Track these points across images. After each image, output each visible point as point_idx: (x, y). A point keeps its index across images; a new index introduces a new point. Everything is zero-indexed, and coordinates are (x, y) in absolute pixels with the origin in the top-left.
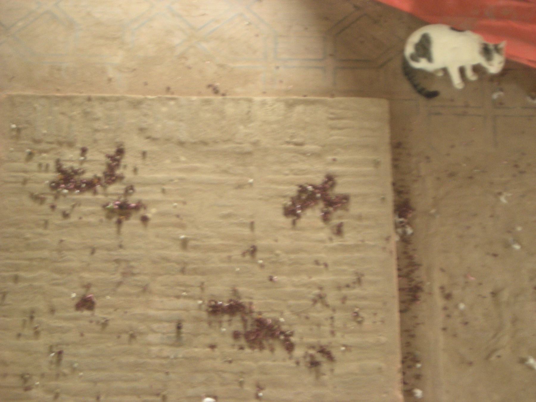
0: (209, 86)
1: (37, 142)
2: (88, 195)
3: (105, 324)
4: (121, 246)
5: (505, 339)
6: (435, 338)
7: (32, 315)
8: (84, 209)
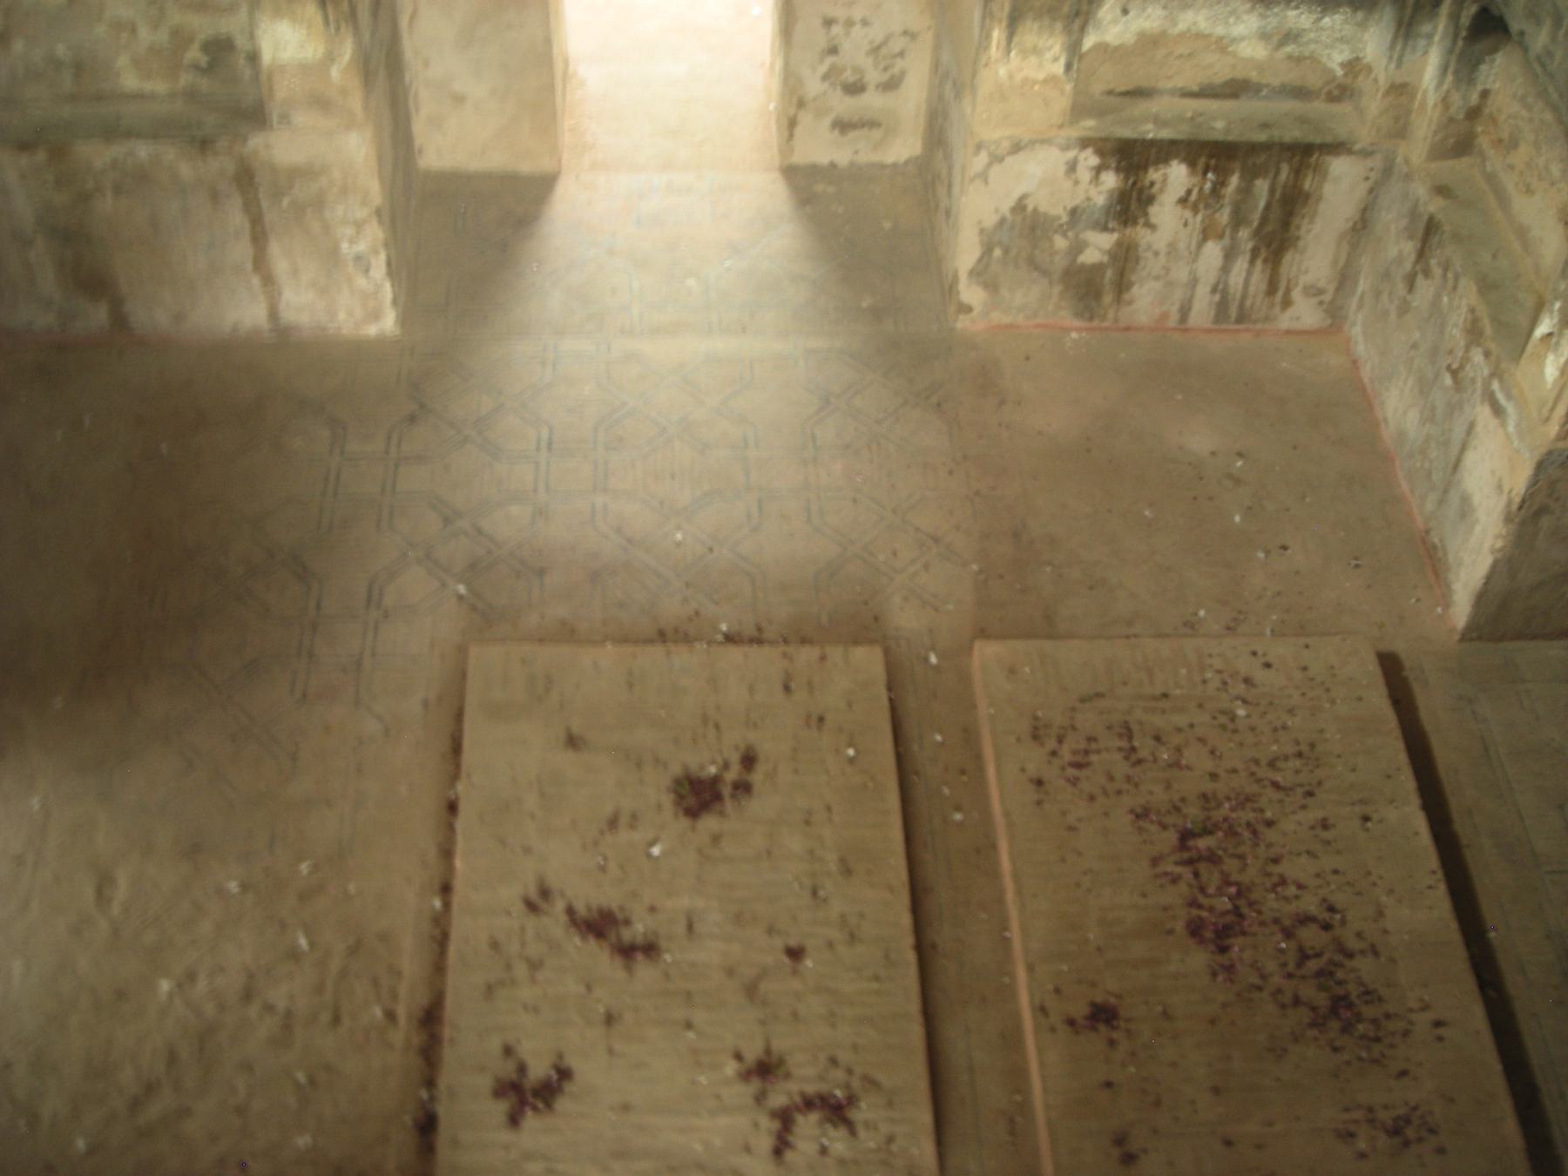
2: (811, 1089)
3: (771, 930)
5: (335, 964)
6: (411, 963)
7: (853, 938)
8: (810, 1071)
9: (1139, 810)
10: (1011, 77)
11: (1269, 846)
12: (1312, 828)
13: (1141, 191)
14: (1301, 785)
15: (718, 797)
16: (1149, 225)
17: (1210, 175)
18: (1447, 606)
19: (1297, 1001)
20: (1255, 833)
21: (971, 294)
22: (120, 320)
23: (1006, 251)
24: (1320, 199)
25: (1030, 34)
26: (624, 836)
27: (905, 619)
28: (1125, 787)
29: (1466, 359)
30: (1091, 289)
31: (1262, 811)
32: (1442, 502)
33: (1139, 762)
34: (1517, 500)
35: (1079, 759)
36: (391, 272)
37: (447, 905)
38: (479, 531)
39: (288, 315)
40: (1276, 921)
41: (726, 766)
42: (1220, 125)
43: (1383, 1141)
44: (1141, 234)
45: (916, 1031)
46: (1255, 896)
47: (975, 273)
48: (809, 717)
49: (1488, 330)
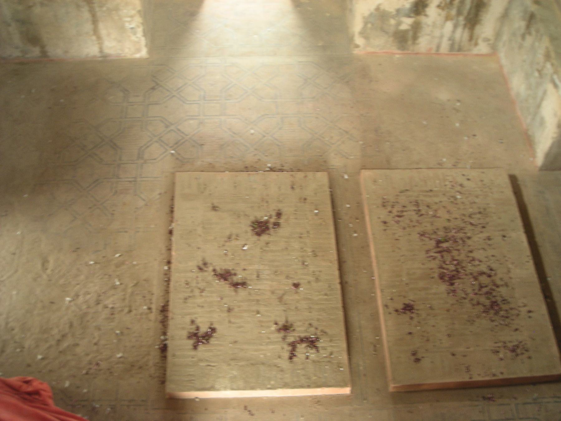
0: (252, 415)
1: (329, 362)
2: (303, 335)
4: (284, 311)
5: (129, 290)
6: (157, 290)
7: (317, 280)
8: (302, 329)
9: (422, 233)
11: (469, 246)
12: (485, 240)
14: (480, 224)
15: (267, 228)
16: (426, 15)
18: (534, 156)
19: (478, 303)
20: (464, 241)
21: (359, 41)
22: (44, 53)
23: (373, 24)
26: (234, 243)
27: (336, 162)
28: (417, 224)
29: (544, 67)
30: (403, 39)
31: (465, 233)
33: (422, 215)
35: (399, 214)
36: (145, 35)
37: (169, 268)
38: (179, 130)
39: (107, 51)
40: (471, 274)
41: (270, 217)
43: (509, 354)
44: (422, 19)
45: (341, 314)
46: (464, 265)
48: (300, 199)
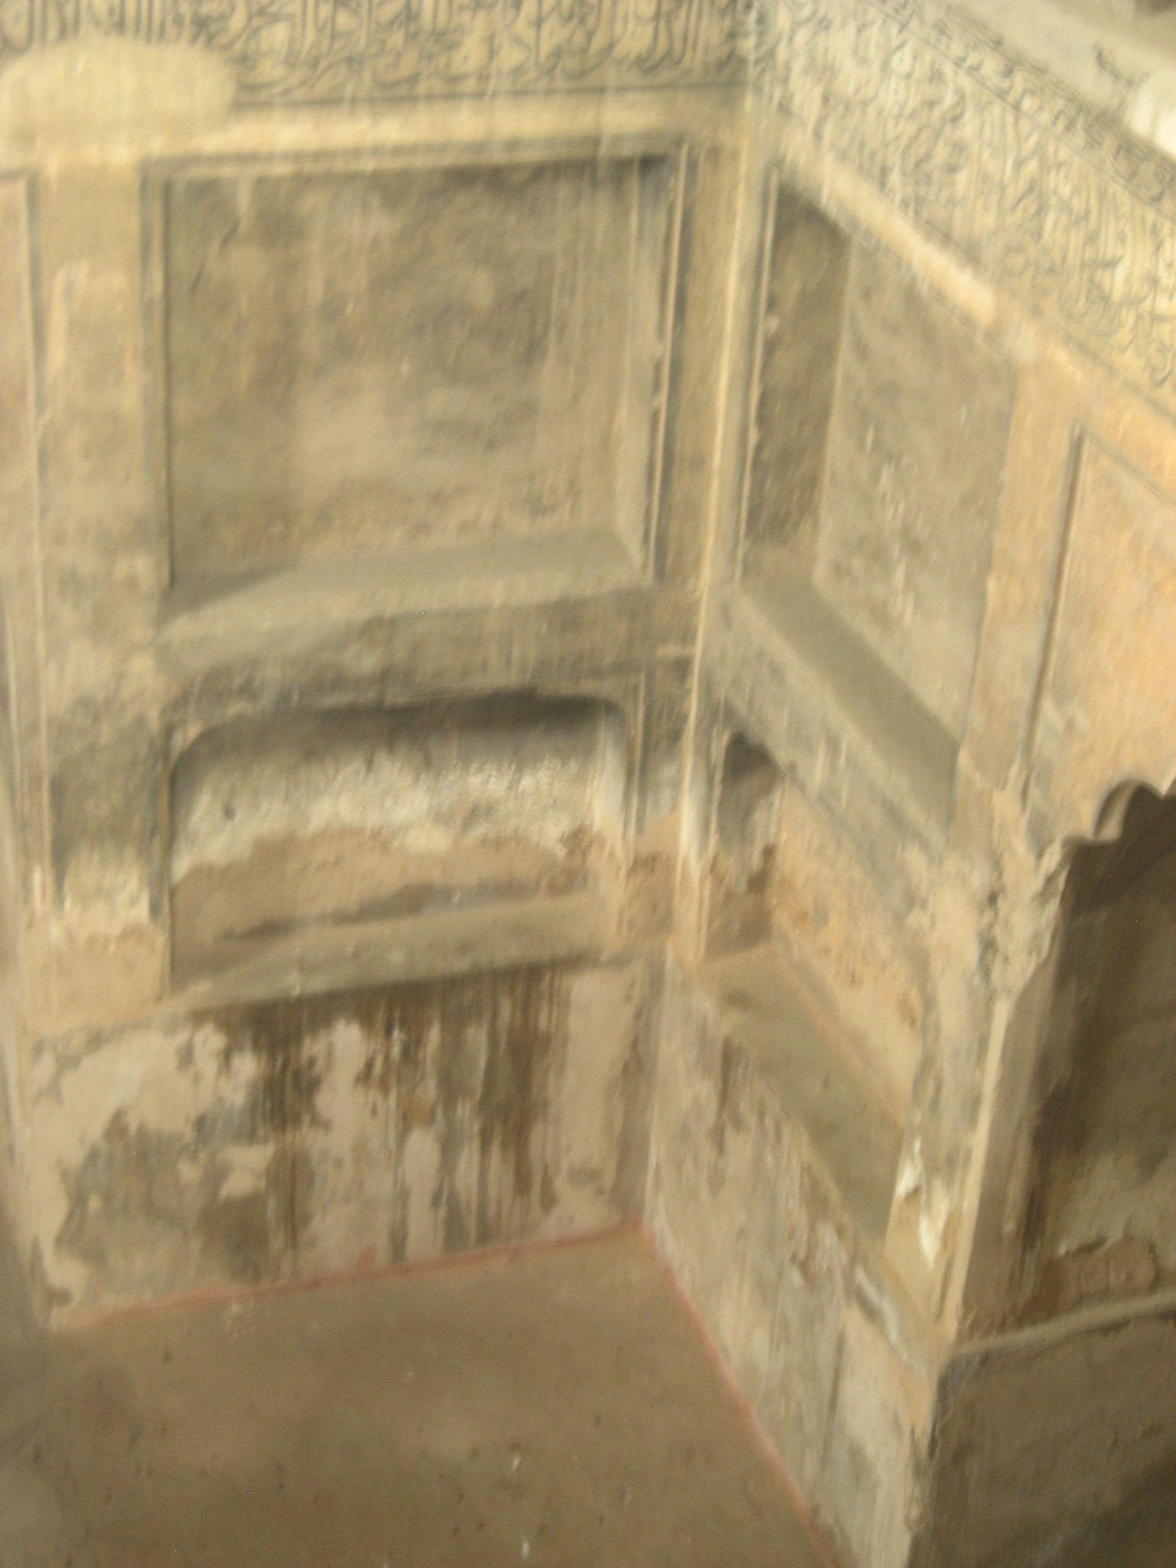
10: (70, 936)
13: (297, 1077)
16: (316, 1121)
17: (396, 1034)
21: (65, 1272)
23: (108, 1199)
24: (565, 1041)
25: (87, 869)
30: (246, 1234)
32: (825, 1460)
34: (924, 1443)
42: (397, 958)
44: (310, 1138)
47: (60, 1240)
49: (835, 1196)
